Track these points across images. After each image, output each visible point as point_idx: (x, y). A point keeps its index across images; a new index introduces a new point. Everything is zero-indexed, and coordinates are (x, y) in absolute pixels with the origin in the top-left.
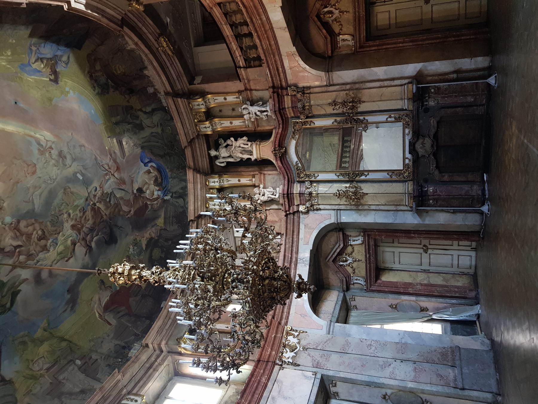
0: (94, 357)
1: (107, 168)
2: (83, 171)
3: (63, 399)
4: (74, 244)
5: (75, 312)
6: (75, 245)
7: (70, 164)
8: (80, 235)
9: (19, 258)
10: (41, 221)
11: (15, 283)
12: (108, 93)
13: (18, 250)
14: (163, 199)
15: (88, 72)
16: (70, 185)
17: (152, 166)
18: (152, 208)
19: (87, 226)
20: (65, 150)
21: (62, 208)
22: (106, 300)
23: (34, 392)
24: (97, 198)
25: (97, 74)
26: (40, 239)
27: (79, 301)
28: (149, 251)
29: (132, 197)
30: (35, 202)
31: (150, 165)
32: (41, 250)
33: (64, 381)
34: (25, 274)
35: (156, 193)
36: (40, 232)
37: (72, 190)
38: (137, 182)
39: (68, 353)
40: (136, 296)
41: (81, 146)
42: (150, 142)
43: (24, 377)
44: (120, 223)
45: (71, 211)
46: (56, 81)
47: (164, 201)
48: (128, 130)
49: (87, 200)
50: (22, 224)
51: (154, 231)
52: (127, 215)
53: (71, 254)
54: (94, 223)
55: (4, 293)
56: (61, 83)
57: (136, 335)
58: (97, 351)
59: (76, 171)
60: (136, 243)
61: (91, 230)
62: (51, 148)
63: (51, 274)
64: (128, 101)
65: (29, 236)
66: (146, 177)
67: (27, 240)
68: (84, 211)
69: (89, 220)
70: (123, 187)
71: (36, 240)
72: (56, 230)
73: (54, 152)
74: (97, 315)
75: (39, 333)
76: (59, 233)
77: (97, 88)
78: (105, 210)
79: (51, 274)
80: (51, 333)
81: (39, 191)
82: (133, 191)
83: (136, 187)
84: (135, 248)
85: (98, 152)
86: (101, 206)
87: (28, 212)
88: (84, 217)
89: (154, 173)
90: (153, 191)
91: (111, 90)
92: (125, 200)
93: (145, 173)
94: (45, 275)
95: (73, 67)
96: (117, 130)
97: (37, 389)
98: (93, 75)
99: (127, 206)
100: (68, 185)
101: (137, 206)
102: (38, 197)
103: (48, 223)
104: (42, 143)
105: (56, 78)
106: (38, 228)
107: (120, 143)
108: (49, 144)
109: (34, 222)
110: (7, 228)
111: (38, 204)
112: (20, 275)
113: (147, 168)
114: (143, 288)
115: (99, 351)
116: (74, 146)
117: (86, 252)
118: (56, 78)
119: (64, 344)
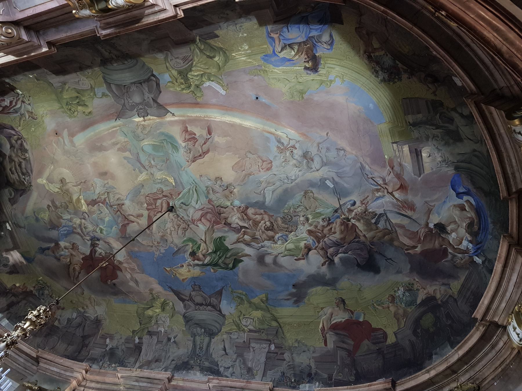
0: (287, 356)
1: (380, 182)
2: (337, 179)
3: (238, 360)
4: (309, 249)
5: (298, 306)
6: (310, 250)
7: (318, 168)
8: (319, 242)
9: (244, 236)
10: (271, 214)
11: (239, 253)
12: (400, 79)
13: (243, 230)
14: (471, 257)
15: (365, 52)
16: (314, 190)
17: (468, 201)
18: (452, 260)
19: (331, 238)
20: (313, 151)
21: (298, 210)
22: (340, 320)
23: (232, 336)
24: (354, 213)
25: (377, 54)
26: (267, 229)
27: (306, 300)
28: (422, 309)
29: (422, 232)
30: (266, 195)
31: (465, 198)
32: (268, 239)
33: (251, 349)
34: (248, 250)
35: (465, 243)
36: (268, 224)
37: (316, 195)
38: (439, 214)
39: (272, 332)
40: (374, 343)
41: (338, 150)
42: (469, 163)
43: (233, 321)
44: (390, 253)
45: (310, 217)
46: (314, 69)
47: (473, 262)
48: (434, 137)
49: (336, 211)
50: (250, 211)
51: (442, 292)
52: (407, 250)
53: (303, 256)
54: (343, 239)
55: (227, 256)
56: (322, 71)
57: (330, 378)
58: (292, 354)
59: (325, 176)
60: (409, 289)
61: (337, 244)
62: (294, 147)
63: (275, 262)
64: (434, 93)
65: (256, 223)
66: (456, 214)
67: (254, 225)
68: (329, 222)
69: (335, 233)
70: (409, 213)
71: (263, 228)
72: (287, 228)
73: (298, 153)
74: (321, 326)
75: (256, 300)
76: (291, 232)
77: (380, 73)
78: (365, 230)
79: (275, 262)
80: (267, 307)
81: (272, 188)
82: (428, 224)
83: (434, 219)
84: (407, 294)
85: (368, 160)
86: (360, 225)
87: (256, 203)
88: (329, 228)
89: (472, 214)
90: (460, 237)
91: (405, 76)
92: (409, 230)
93: (455, 206)
94: (269, 259)
95: (341, 46)
96: (416, 134)
97: (234, 337)
98: (372, 55)
99: (410, 238)
100: (310, 189)
101: (429, 246)
102: (271, 193)
103: (279, 219)
104: (282, 141)
105: (314, 64)
106: (267, 219)
107: (416, 154)
108: (292, 143)
109: (263, 213)
110: (235, 209)
111: (269, 199)
112: (244, 250)
113: (459, 201)
114: (387, 344)
115: (294, 355)
116: (328, 149)
117: (325, 263)
118: (314, 64)
119: (274, 324)
